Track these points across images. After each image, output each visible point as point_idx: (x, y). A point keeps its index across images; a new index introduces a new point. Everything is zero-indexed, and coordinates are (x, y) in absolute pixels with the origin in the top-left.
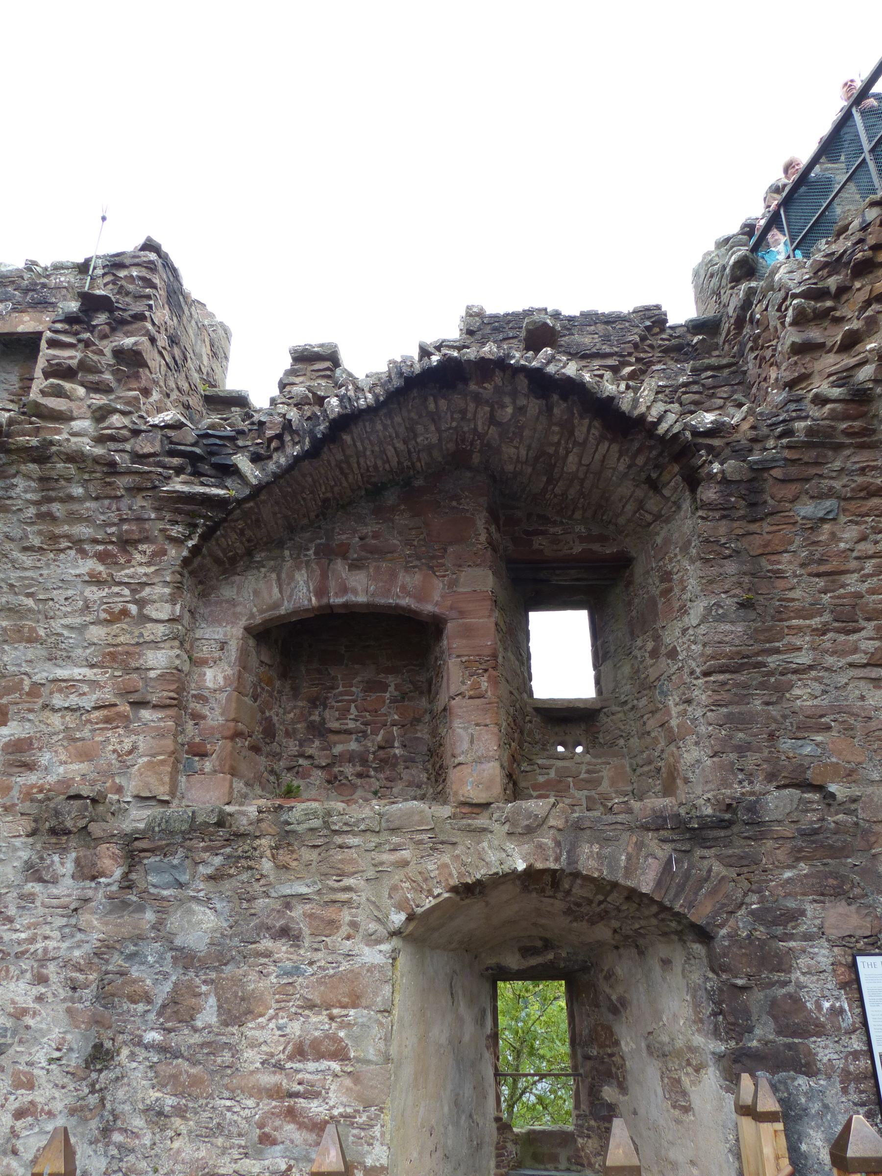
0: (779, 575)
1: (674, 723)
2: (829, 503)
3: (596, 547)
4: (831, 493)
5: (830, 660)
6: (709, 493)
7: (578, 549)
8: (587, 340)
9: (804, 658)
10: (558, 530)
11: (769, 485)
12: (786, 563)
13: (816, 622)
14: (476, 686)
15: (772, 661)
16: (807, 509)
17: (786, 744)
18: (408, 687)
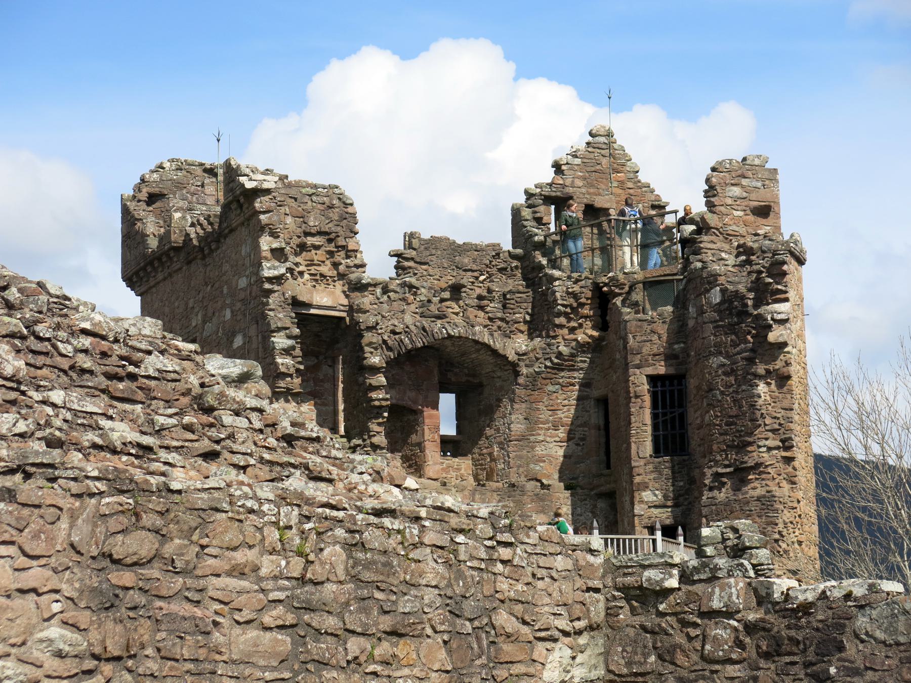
0: (538, 409)
1: (495, 453)
2: (557, 387)
3: (471, 379)
4: (558, 384)
5: (548, 439)
6: (521, 380)
7: (464, 379)
8: (466, 261)
9: (541, 438)
10: (458, 370)
11: (540, 380)
12: (541, 406)
13: (546, 426)
14: (433, 438)
15: (532, 438)
16: (551, 388)
17: (532, 466)
18: (393, 428)
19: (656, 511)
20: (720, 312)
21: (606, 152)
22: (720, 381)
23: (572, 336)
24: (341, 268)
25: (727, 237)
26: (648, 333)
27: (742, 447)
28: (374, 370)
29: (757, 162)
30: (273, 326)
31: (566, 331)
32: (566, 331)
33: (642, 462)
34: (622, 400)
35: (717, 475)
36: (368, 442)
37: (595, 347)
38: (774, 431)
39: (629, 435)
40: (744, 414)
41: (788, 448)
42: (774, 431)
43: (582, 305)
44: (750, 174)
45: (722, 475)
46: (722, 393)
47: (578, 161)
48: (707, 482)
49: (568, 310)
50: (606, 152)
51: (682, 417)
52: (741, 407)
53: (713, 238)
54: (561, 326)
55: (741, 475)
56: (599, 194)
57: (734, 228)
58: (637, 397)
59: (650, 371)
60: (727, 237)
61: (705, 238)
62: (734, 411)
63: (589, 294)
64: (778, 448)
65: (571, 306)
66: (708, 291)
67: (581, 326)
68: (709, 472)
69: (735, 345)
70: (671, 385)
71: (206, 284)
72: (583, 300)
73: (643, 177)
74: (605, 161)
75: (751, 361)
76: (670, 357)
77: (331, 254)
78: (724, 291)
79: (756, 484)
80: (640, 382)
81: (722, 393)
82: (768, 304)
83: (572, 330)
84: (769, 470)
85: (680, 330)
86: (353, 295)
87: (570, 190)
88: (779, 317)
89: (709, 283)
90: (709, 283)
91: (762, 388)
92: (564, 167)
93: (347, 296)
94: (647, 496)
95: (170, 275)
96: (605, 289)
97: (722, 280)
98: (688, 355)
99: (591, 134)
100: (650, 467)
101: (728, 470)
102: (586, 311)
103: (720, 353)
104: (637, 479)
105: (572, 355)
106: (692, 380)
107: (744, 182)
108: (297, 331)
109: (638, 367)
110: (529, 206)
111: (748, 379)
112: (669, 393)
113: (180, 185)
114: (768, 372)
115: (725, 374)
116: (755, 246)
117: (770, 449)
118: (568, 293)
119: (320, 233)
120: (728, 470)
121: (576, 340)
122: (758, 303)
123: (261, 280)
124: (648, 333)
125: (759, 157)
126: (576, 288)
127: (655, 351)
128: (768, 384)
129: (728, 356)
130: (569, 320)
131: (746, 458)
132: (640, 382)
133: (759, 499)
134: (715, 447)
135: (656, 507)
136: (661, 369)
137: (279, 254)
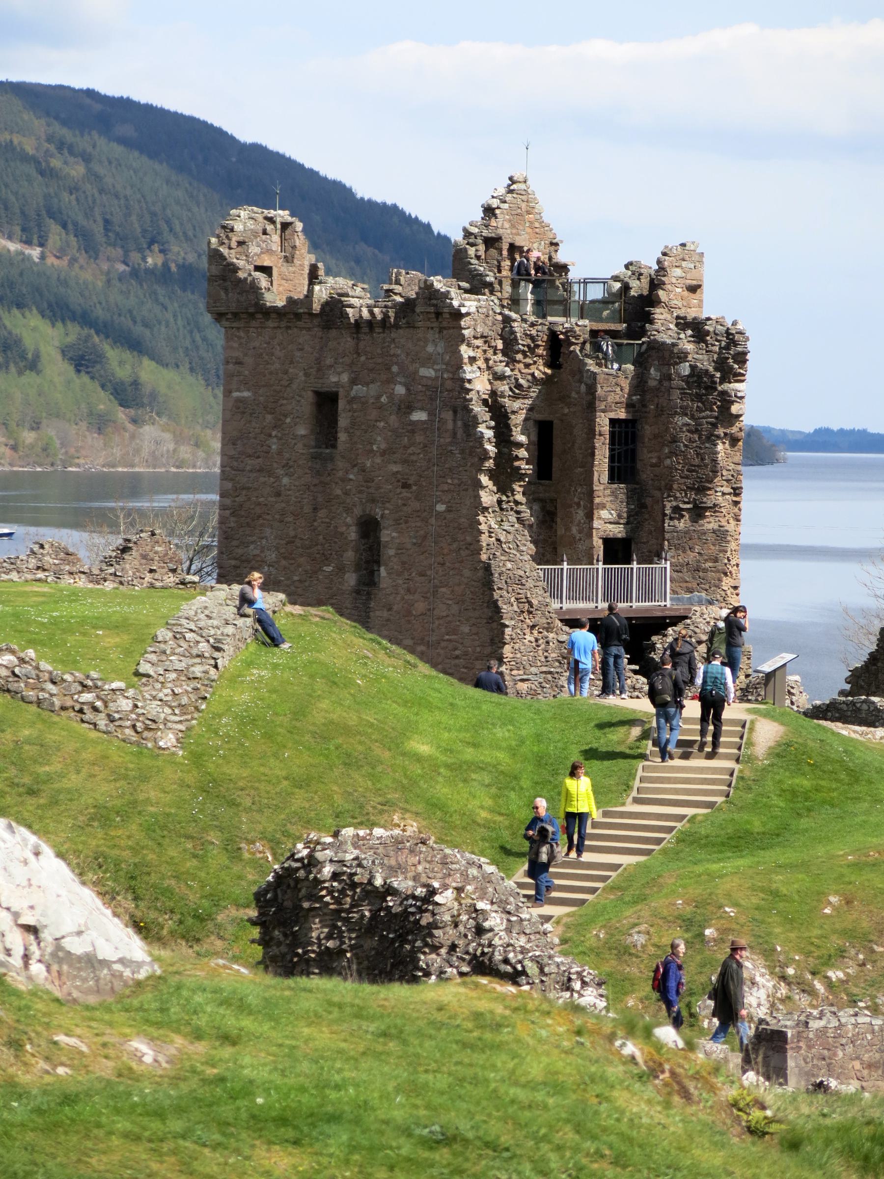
19: (610, 526)
20: (687, 383)
21: (524, 198)
22: (684, 436)
23: (526, 371)
24: (491, 362)
25: (670, 309)
26: (613, 385)
27: (702, 490)
28: (519, 445)
29: (692, 248)
30: (480, 420)
31: (521, 366)
32: (521, 366)
33: (602, 487)
34: (579, 432)
35: (676, 509)
36: (511, 499)
37: (547, 382)
38: (728, 481)
39: (592, 465)
40: (706, 466)
41: (737, 495)
42: (728, 481)
43: (538, 346)
44: (687, 258)
45: (683, 510)
46: (685, 446)
47: (506, 206)
48: (667, 512)
49: (526, 349)
50: (524, 198)
51: (633, 452)
52: (703, 459)
53: (662, 310)
54: (519, 362)
55: (698, 512)
56: (519, 234)
57: (675, 302)
58: (600, 435)
59: (612, 415)
60: (670, 309)
61: (658, 310)
62: (697, 461)
63: (545, 338)
64: (730, 494)
65: (529, 346)
66: (677, 364)
67: (535, 363)
68: (668, 505)
69: (699, 410)
70: (627, 427)
71: (359, 354)
72: (540, 343)
73: (546, 219)
74: (524, 205)
75: (714, 426)
76: (629, 406)
77: (485, 351)
78: (693, 368)
79: (711, 519)
80: (603, 423)
81: (685, 446)
82: (730, 382)
83: (527, 366)
84: (722, 510)
85: (639, 384)
86: (496, 383)
87: (500, 231)
88: (739, 394)
89: (679, 358)
90: (679, 358)
91: (720, 447)
92: (497, 211)
93: (491, 383)
94: (604, 514)
95: (288, 328)
96: (561, 337)
97: (690, 358)
98: (644, 406)
99: (511, 179)
100: (608, 492)
101: (688, 506)
102: (540, 351)
103: (686, 415)
104: (597, 500)
105: (529, 387)
106: (647, 427)
107: (684, 264)
108: (493, 423)
109: (604, 411)
110: (472, 245)
111: (712, 439)
112: (624, 434)
113: (255, 234)
114: (726, 434)
115: (689, 431)
116: (711, 329)
117: (724, 494)
118: (526, 335)
119: (482, 337)
120: (688, 506)
121: (533, 375)
122: (723, 380)
123: (463, 380)
124: (613, 385)
125: (693, 243)
126: (534, 332)
127: (618, 400)
128: (724, 443)
129: (692, 417)
130: (525, 356)
131: (705, 500)
132: (603, 423)
133: (714, 532)
134: (675, 486)
135: (610, 523)
136: (622, 415)
137: (472, 360)
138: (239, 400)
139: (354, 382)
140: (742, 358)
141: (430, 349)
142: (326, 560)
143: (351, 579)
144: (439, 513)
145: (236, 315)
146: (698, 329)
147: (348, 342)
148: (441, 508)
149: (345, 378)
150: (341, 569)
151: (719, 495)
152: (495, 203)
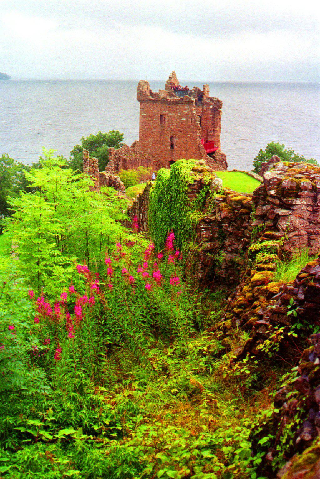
27: (214, 127)
138: (143, 115)
139: (169, 113)
140: (222, 105)
141: (186, 107)
142: (163, 144)
143: (169, 147)
144: (188, 137)
145: (143, 100)
146: (211, 99)
147: (167, 105)
148: (189, 136)
149: (167, 112)
150: (167, 146)
151: (218, 129)
152: (171, 76)
